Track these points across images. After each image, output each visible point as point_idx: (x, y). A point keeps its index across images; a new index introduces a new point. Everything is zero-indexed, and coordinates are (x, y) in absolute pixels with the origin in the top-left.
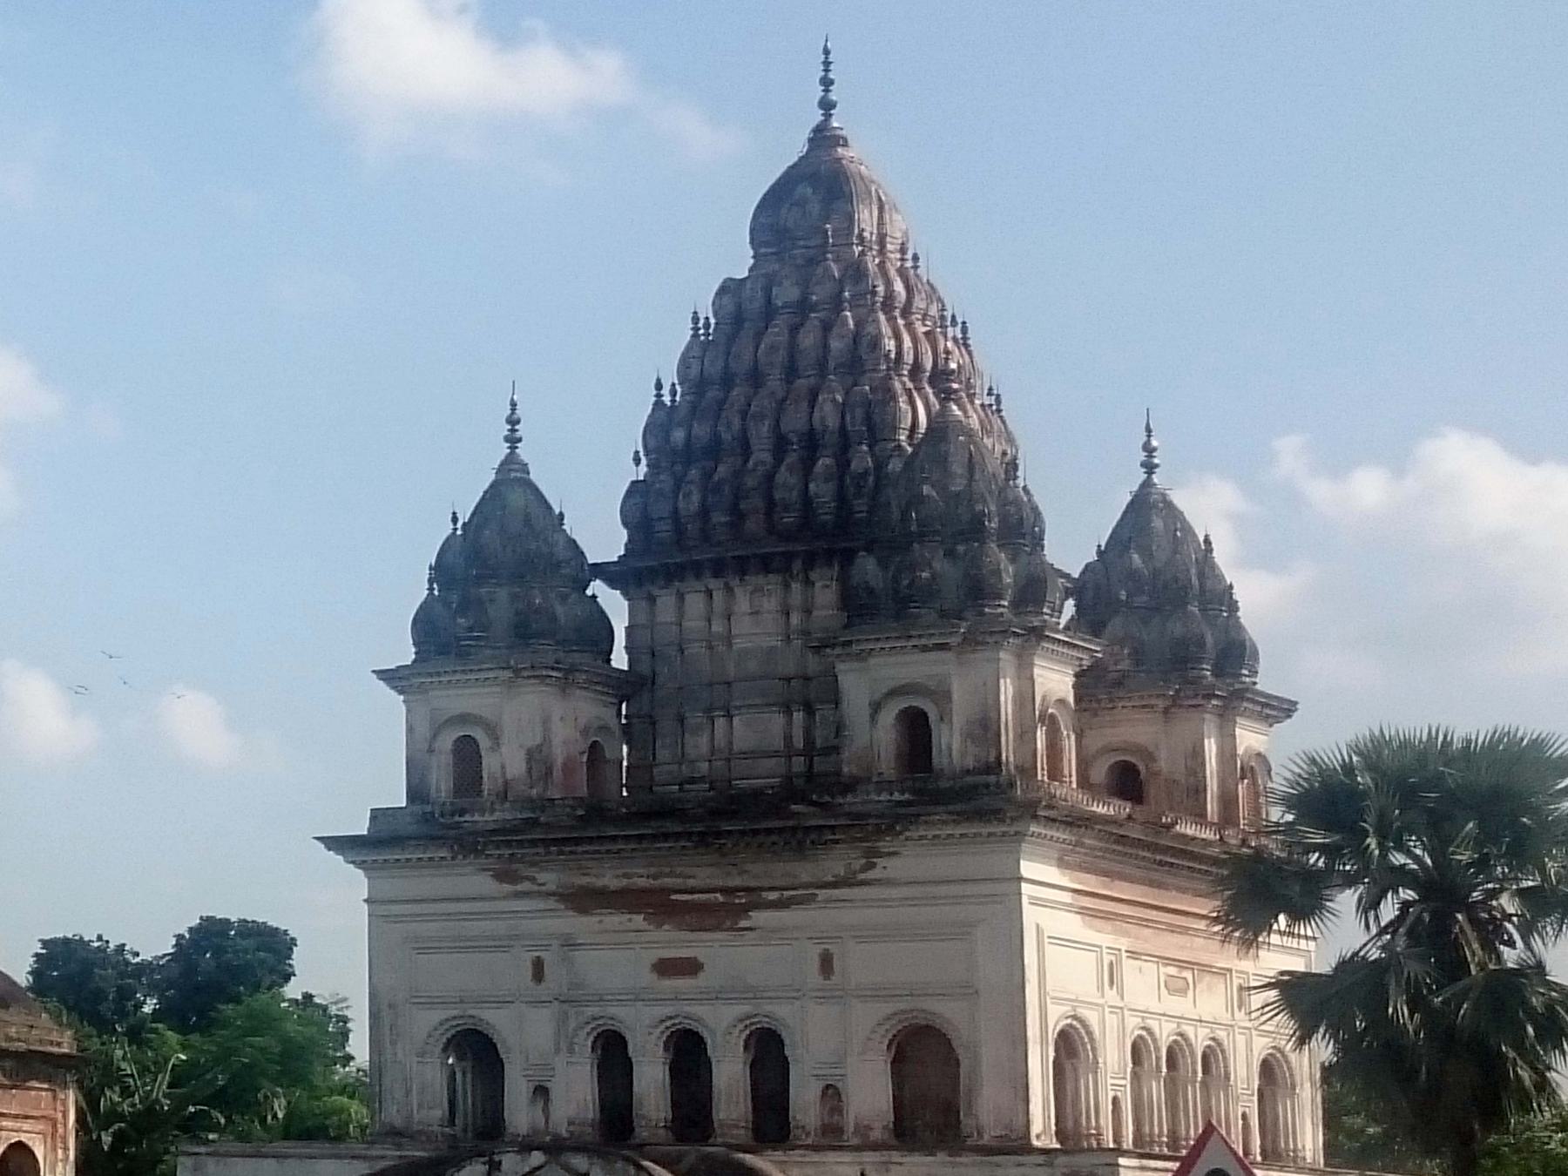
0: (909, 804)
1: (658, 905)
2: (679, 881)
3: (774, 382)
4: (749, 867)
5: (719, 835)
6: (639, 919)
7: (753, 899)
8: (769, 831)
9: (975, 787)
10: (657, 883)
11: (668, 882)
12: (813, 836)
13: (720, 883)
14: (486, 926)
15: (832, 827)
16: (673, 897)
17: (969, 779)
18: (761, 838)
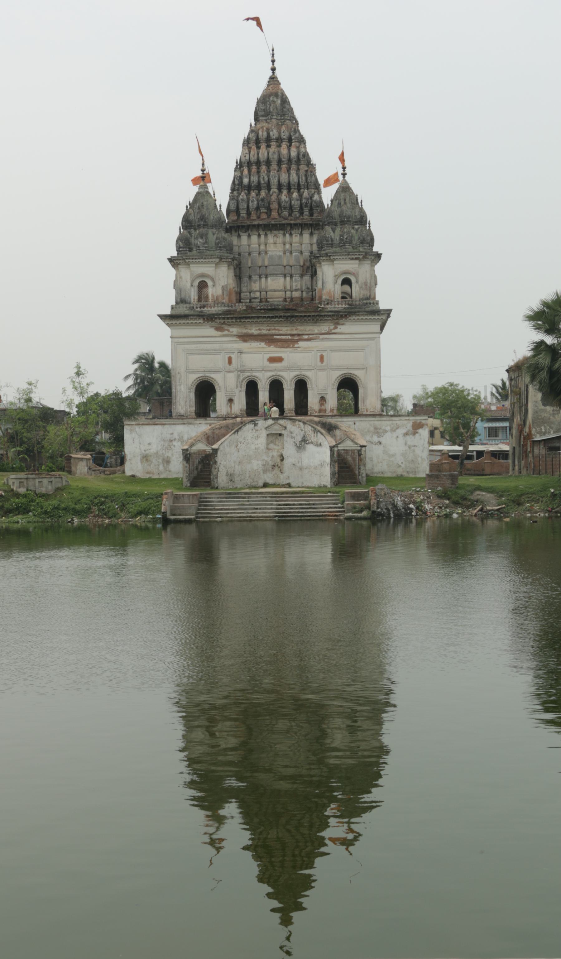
0: (348, 308)
1: (269, 340)
2: (277, 331)
3: (274, 166)
4: (299, 327)
5: (293, 317)
6: (263, 344)
7: (299, 338)
8: (309, 316)
9: (367, 303)
10: (270, 332)
11: (274, 332)
12: (321, 318)
13: (289, 332)
14: (209, 346)
15: (328, 315)
16: (275, 337)
17: (365, 301)
18: (305, 318)
